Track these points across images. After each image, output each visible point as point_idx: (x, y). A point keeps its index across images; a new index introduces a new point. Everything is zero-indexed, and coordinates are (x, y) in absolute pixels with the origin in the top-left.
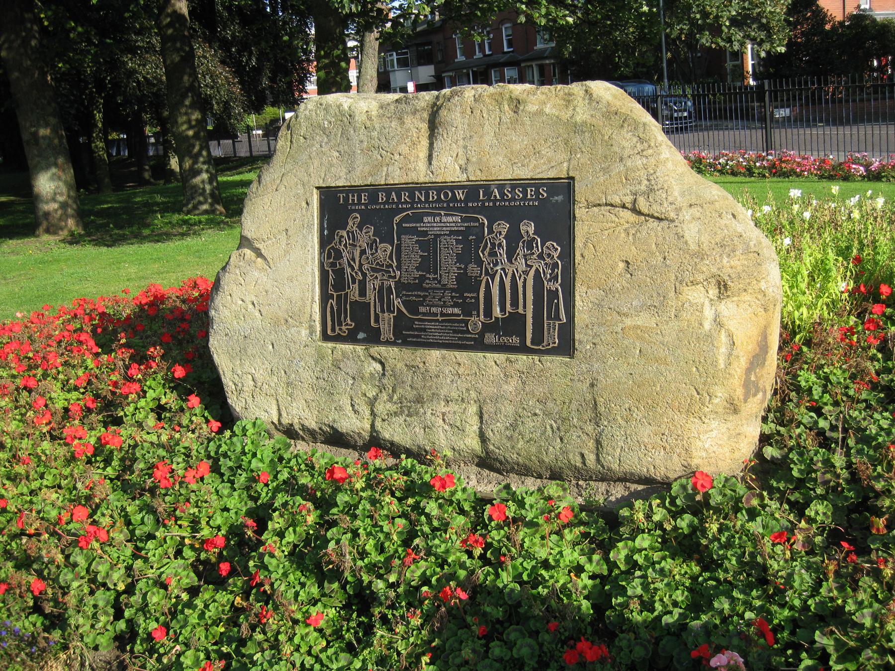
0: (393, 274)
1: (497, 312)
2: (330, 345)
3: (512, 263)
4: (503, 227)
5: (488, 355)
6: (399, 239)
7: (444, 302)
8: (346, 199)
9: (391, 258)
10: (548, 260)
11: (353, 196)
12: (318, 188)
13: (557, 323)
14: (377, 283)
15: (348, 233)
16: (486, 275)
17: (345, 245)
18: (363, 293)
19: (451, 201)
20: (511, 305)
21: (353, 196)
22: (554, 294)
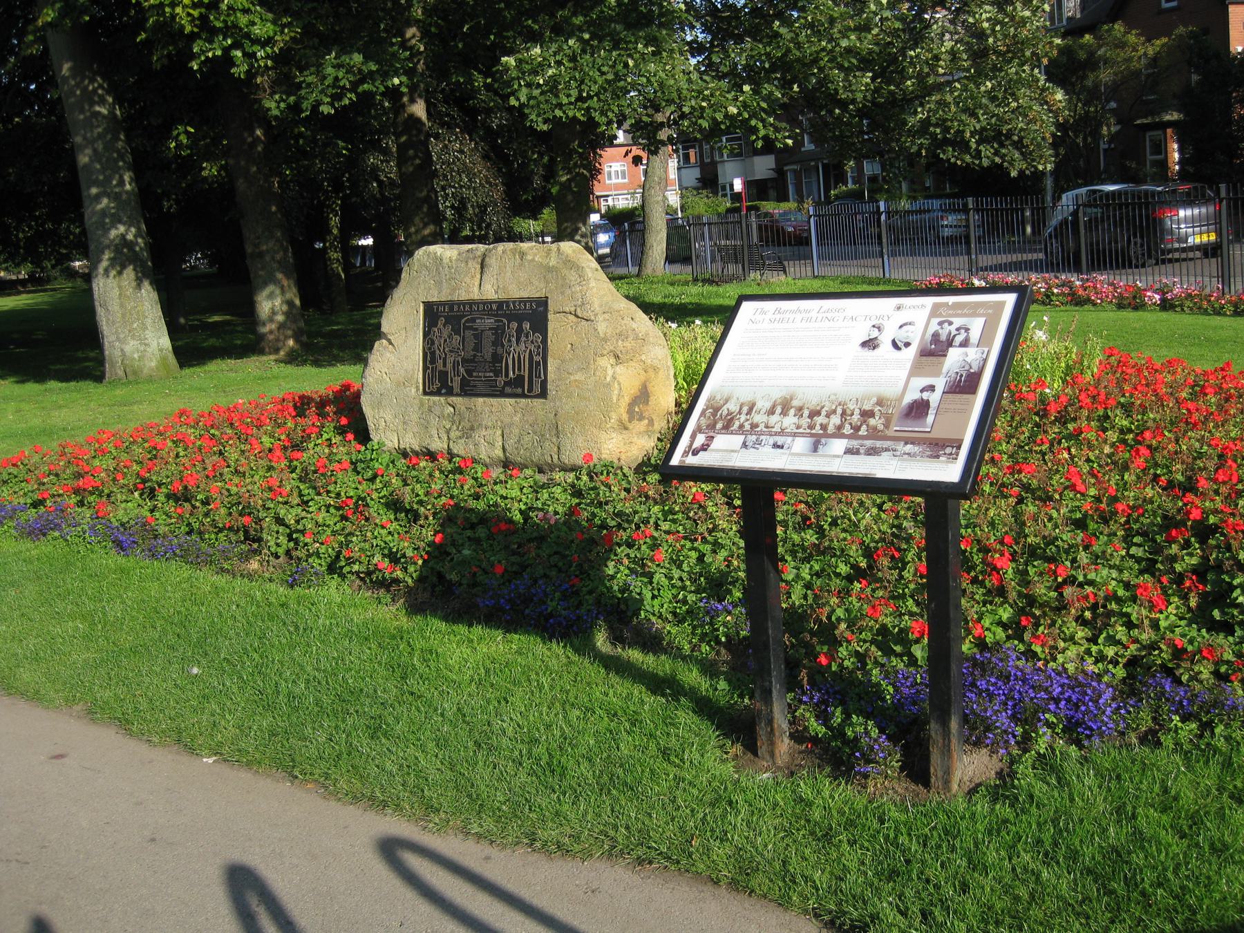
4: (515, 325)
18: (445, 365)
22: (538, 363)
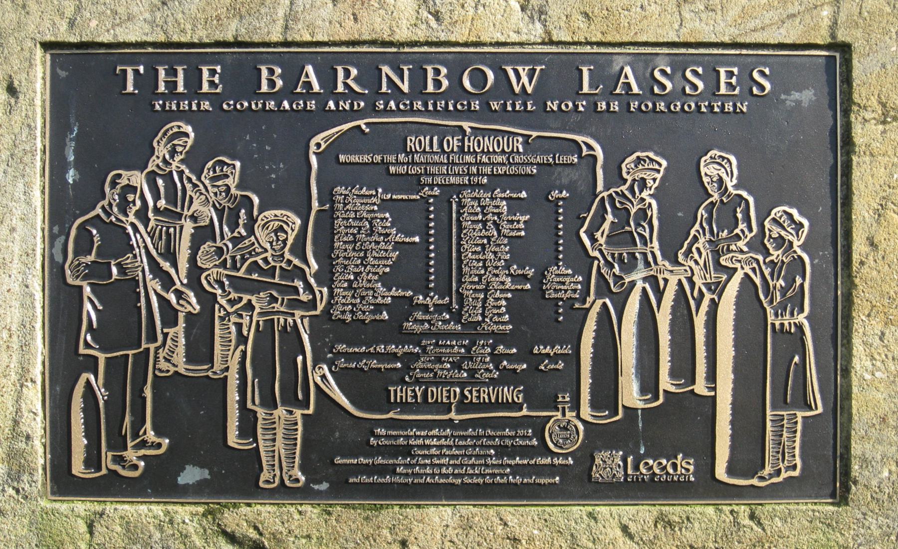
0: (304, 297)
1: (631, 394)
2: (82, 506)
3: (676, 263)
4: (650, 169)
5: (603, 510)
6: (327, 196)
7: (472, 372)
8: (147, 81)
9: (299, 249)
10: (776, 254)
11: (172, 72)
12: (47, 46)
13: (800, 414)
14: (251, 324)
15: (151, 178)
16: (599, 295)
17: (142, 215)
18: (200, 347)
19: (495, 93)
20: (673, 374)
21: (172, 72)
22: (793, 340)
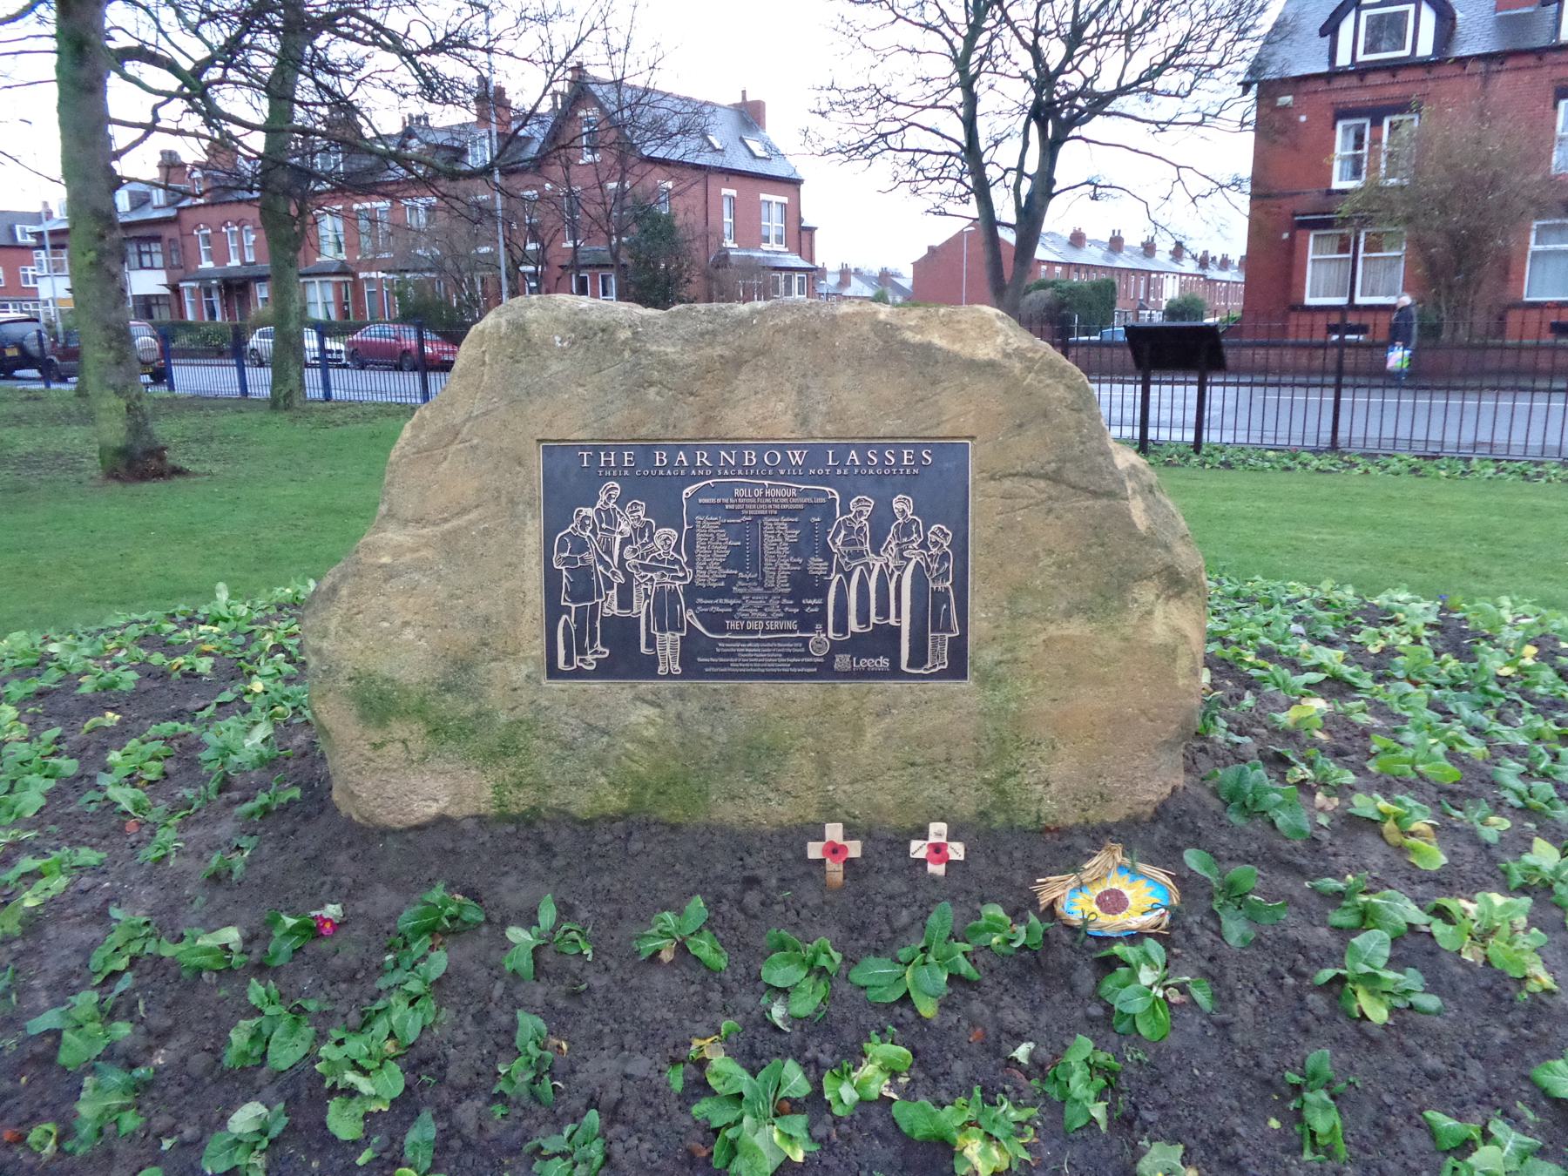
1: (853, 625)
4: (862, 506)
10: (934, 551)
13: (947, 636)
17: (593, 531)
18: (626, 602)
22: (941, 597)
